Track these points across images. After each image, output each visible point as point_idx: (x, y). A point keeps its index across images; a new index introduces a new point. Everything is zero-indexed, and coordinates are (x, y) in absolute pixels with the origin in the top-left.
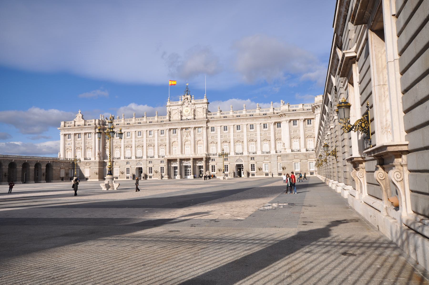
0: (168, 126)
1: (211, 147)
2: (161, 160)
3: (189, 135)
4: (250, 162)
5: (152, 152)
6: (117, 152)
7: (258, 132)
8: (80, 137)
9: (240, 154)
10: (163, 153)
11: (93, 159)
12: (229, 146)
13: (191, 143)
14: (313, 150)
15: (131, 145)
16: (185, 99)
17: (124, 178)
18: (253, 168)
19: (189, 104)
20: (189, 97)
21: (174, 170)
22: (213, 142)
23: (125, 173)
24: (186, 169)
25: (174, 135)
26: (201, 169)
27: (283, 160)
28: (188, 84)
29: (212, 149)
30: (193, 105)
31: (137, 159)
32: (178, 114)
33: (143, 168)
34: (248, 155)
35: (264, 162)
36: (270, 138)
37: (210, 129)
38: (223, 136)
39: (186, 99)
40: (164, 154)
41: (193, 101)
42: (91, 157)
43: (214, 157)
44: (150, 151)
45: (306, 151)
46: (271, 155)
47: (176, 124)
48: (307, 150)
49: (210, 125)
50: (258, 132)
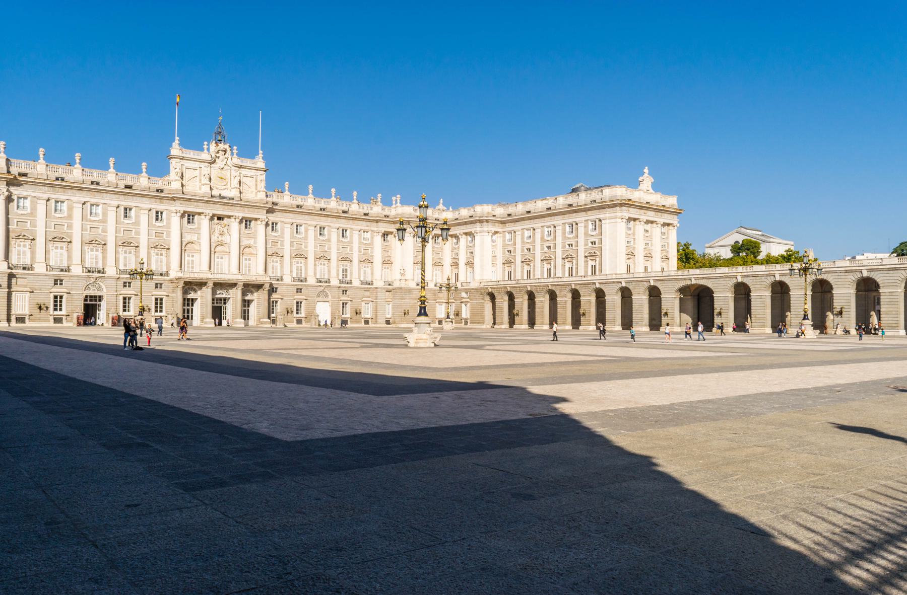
0: (181, 204)
1: (272, 264)
3: (226, 231)
4: (342, 298)
6: (22, 249)
7: (356, 245)
9: (326, 282)
12: (305, 265)
13: (229, 249)
15: (70, 236)
16: (219, 150)
17: (48, 321)
18: (58, 304)
19: (225, 165)
20: (227, 147)
22: (277, 253)
23: (51, 307)
25: (192, 227)
27: (404, 299)
28: (221, 118)
29: (273, 268)
30: (237, 168)
32: (200, 180)
35: (363, 299)
36: (373, 259)
37: (270, 228)
38: (295, 243)
39: (221, 150)
41: (236, 160)
43: (278, 284)
44: (125, 258)
46: (376, 288)
47: (199, 204)
49: (272, 218)
50: (356, 245)
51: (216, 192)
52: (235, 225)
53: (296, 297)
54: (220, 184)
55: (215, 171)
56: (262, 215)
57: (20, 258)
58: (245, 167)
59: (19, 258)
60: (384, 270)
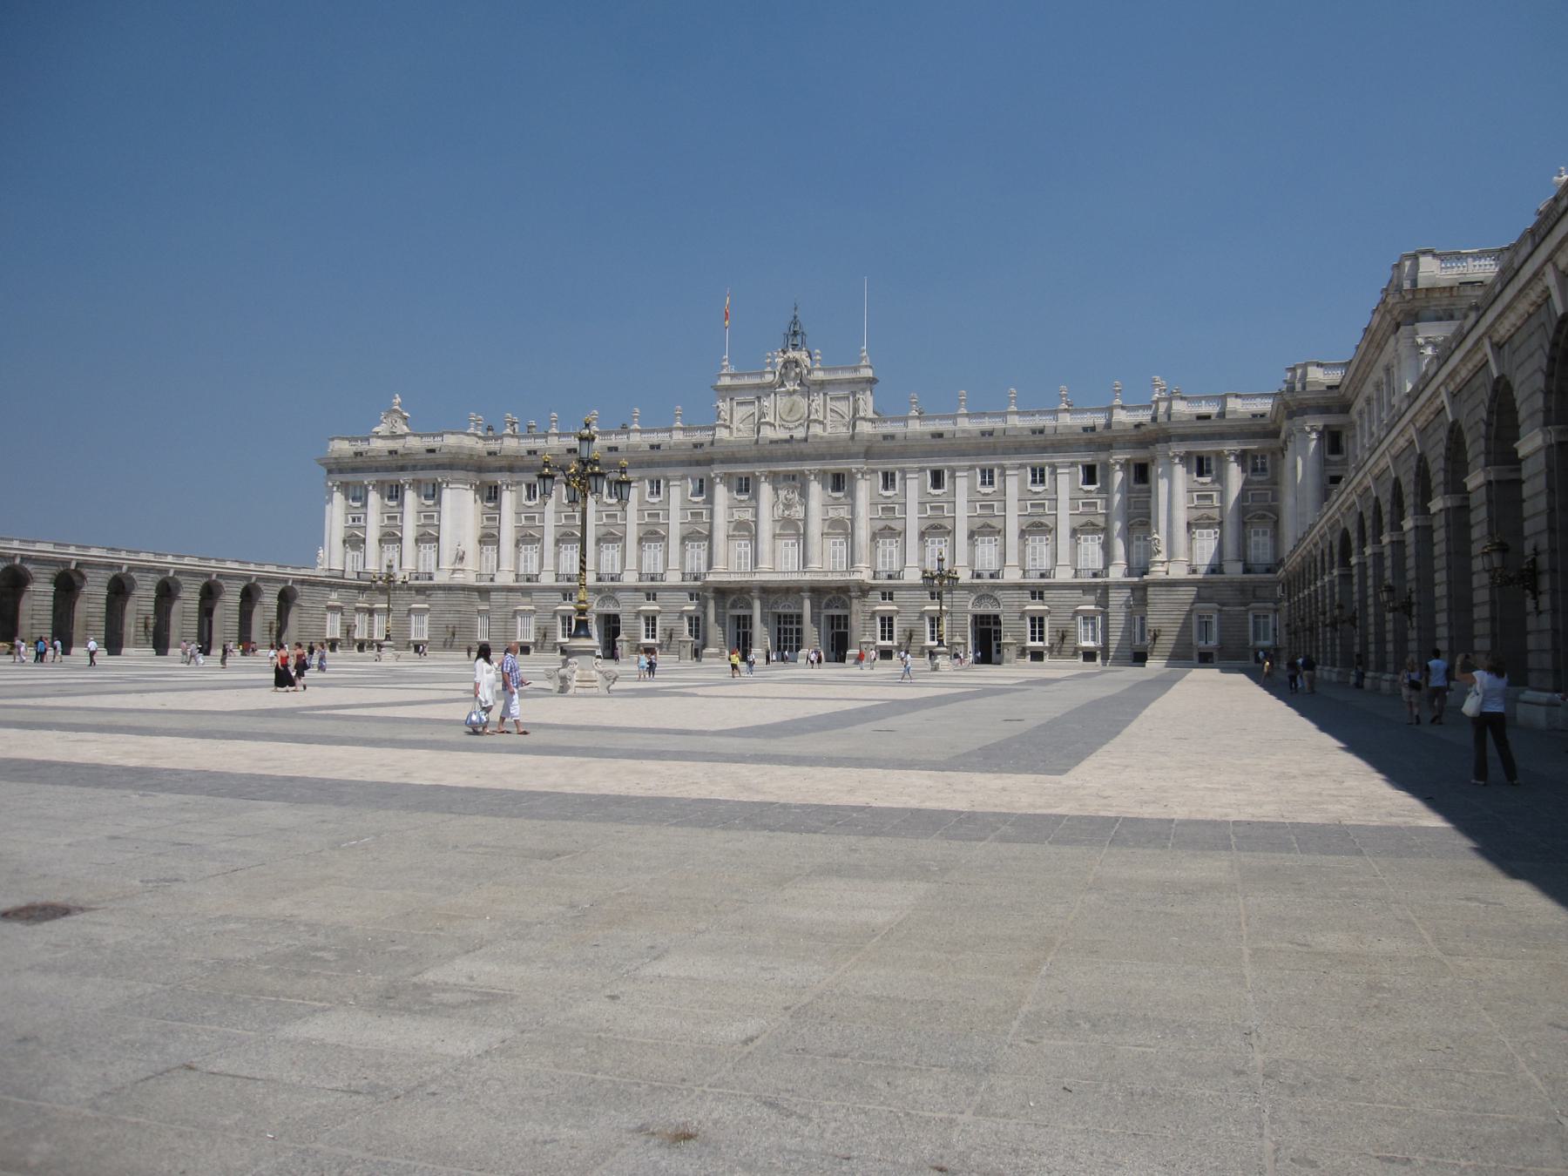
2: (691, 591)
4: (1028, 608)
5: (655, 559)
8: (397, 496)
9: (992, 576)
10: (699, 564)
11: (441, 578)
14: (1268, 571)
21: (738, 627)
22: (891, 529)
24: (782, 626)
26: (839, 626)
29: (884, 556)
30: (818, 387)
31: (600, 584)
33: (621, 617)
34: (1022, 581)
35: (1080, 608)
40: (703, 569)
42: (433, 570)
43: (889, 586)
45: (1244, 573)
48: (1247, 570)
51: (782, 434)
52: (815, 488)
53: (927, 608)
54: (789, 419)
55: (783, 402)
56: (854, 465)
57: (526, 567)
58: (830, 382)
59: (526, 567)
60: (1135, 543)
